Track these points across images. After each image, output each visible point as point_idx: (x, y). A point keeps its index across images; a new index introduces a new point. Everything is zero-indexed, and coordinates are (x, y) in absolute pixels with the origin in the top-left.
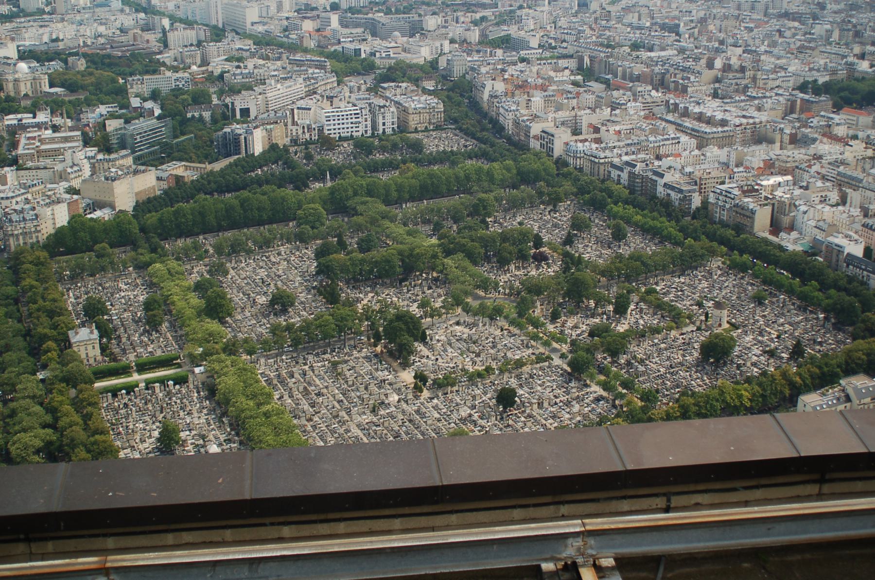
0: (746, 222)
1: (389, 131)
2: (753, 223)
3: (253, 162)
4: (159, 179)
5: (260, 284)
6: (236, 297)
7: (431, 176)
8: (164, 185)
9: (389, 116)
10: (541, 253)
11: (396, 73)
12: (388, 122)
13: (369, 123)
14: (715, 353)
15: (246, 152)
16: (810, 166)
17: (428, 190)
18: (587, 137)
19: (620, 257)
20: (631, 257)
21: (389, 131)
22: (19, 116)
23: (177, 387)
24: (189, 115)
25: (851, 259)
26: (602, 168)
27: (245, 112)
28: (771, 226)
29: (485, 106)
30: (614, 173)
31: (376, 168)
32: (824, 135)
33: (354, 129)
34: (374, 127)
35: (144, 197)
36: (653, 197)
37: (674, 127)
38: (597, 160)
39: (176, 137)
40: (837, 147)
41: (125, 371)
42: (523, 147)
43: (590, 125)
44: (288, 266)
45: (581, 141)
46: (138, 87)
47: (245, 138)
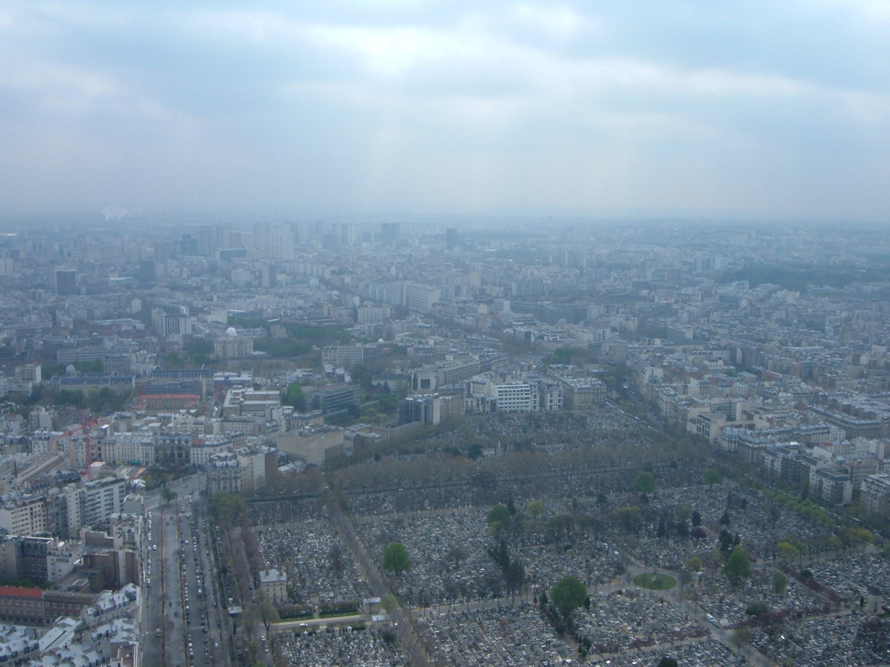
9: (556, 394)
12: (554, 401)
13: (538, 399)
15: (426, 420)
18: (741, 423)
21: (555, 408)
22: (226, 374)
23: (355, 632)
26: (756, 453)
27: (426, 384)
29: (644, 390)
34: (542, 404)
38: (751, 445)
45: (736, 427)
47: (426, 407)
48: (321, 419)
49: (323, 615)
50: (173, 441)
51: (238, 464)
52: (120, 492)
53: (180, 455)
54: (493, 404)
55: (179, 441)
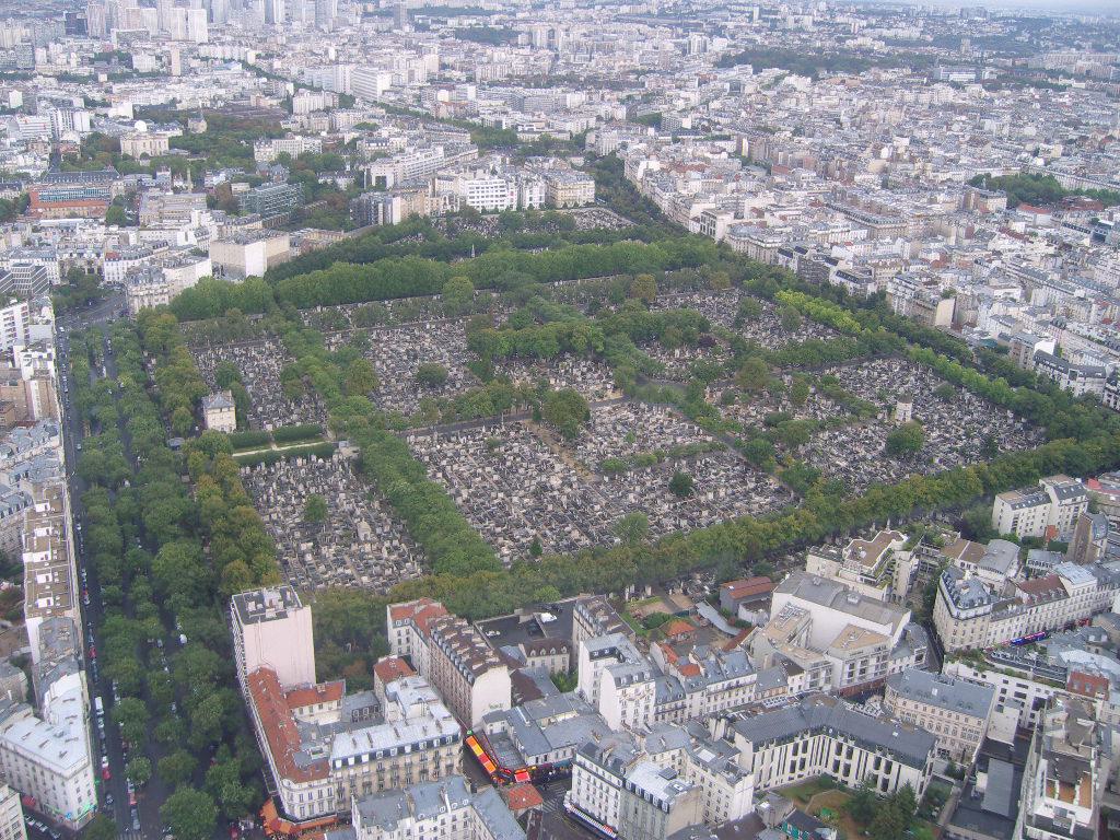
1: (536, 206)
2: (934, 316)
3: (391, 233)
4: (292, 244)
5: (405, 358)
7: (585, 252)
8: (297, 252)
9: (536, 190)
11: (545, 147)
13: (515, 198)
16: (990, 261)
19: (793, 344)
20: (806, 345)
21: (536, 206)
22: (139, 176)
23: (321, 461)
24: (321, 181)
25: (1041, 357)
27: (382, 180)
31: (524, 245)
32: (1002, 230)
35: (275, 263)
36: (827, 285)
37: (842, 215)
39: (308, 203)
40: (1018, 244)
41: (264, 441)
42: (681, 231)
43: (754, 210)
44: (437, 344)
48: (259, 225)
52: (23, 315)
53: (91, 271)
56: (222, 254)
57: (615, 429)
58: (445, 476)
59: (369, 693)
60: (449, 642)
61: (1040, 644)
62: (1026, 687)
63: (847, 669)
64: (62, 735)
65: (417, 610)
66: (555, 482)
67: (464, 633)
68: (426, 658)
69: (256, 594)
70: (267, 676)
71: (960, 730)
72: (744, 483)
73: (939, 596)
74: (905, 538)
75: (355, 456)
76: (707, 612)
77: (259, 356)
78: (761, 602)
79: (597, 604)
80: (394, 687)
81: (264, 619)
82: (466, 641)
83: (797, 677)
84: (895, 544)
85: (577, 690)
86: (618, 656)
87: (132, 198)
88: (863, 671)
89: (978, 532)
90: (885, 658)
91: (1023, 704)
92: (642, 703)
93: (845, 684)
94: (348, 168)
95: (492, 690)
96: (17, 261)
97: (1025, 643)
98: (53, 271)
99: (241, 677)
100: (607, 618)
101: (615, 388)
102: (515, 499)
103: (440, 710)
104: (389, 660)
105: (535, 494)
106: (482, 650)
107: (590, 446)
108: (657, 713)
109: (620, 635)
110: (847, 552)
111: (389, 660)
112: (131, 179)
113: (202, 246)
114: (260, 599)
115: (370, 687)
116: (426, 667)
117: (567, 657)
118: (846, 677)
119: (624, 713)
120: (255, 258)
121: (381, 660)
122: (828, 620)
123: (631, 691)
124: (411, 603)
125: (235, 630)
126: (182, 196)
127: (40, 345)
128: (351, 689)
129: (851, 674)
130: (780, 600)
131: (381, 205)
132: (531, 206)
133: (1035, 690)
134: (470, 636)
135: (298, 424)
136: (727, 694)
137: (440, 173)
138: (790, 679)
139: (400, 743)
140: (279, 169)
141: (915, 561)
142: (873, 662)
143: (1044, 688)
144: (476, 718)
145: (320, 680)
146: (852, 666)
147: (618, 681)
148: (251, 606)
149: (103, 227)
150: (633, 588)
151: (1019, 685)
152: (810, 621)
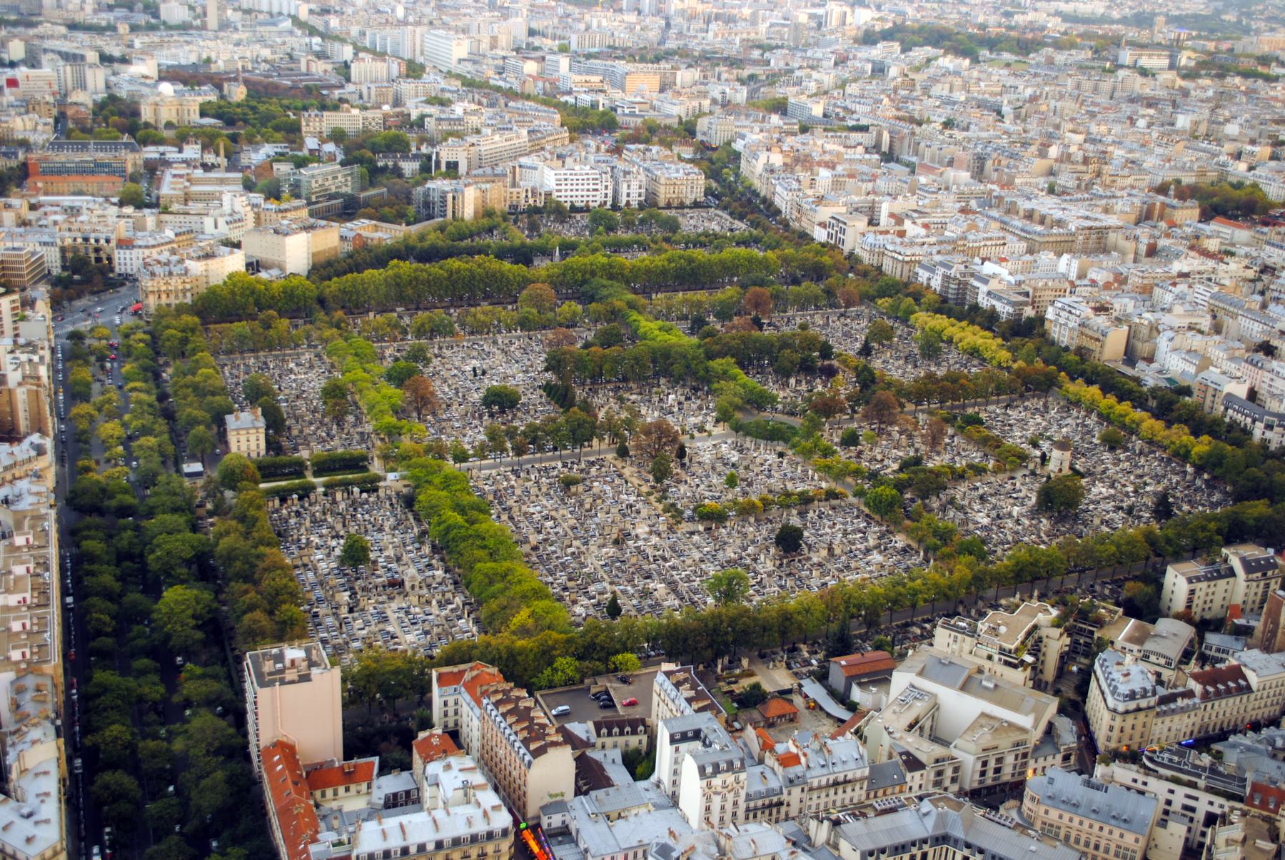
0: (1093, 346)
4: (343, 238)
5: (471, 377)
6: (441, 390)
7: (690, 260)
8: (348, 247)
9: (635, 185)
10: (831, 366)
11: (650, 133)
12: (632, 192)
13: (610, 192)
14: (1059, 501)
16: (1174, 284)
17: (691, 277)
19: (930, 376)
20: (946, 378)
21: (635, 204)
22: (161, 149)
23: (365, 495)
24: (380, 164)
25: (1230, 400)
27: (453, 166)
28: (1125, 354)
29: (758, 184)
30: (923, 275)
31: (618, 247)
32: (1192, 248)
33: (591, 199)
34: (615, 198)
35: (322, 259)
36: (975, 308)
37: (998, 225)
38: (900, 258)
39: (363, 189)
40: (1211, 263)
42: (805, 237)
43: (892, 215)
45: (881, 233)
46: (315, 126)
47: (454, 198)
49: (316, 474)
50: (86, 240)
51: (187, 271)
53: (98, 260)
54: (548, 194)
55: (97, 241)
56: (258, 246)
57: (714, 468)
58: (511, 518)
59: (406, 774)
60: (504, 715)
61: (1216, 747)
62: (1196, 799)
63: (979, 767)
64: (30, 815)
65: (468, 676)
66: (642, 530)
67: (522, 704)
68: (476, 734)
69: (275, 651)
70: (286, 750)
71: (1113, 849)
72: (865, 539)
73: (1093, 684)
74: (1055, 612)
75: (405, 491)
76: (814, 690)
77: (296, 369)
78: (881, 678)
79: (681, 676)
80: (434, 768)
81: (283, 682)
82: (523, 715)
83: (917, 774)
84: (1041, 618)
85: (654, 778)
86: (704, 744)
87: (153, 170)
88: (997, 771)
89: (1147, 609)
90: (1025, 755)
91: (1191, 820)
92: (730, 797)
93: (976, 785)
94: (414, 150)
95: (552, 772)
96: (9, 245)
97: (1203, 742)
98: (53, 259)
99: (253, 750)
100: (692, 693)
101: (718, 421)
102: (592, 548)
103: (489, 798)
104: (432, 736)
105: (616, 542)
106: (543, 726)
107: (683, 488)
108: (748, 810)
109: (708, 714)
110: (982, 626)
111: (432, 736)
112: (151, 152)
113: (235, 236)
114: (280, 658)
115: (406, 766)
116: (476, 744)
117: (644, 738)
118: (977, 777)
119: (708, 809)
120: (297, 251)
121: (422, 735)
122: (961, 707)
123: (717, 781)
124: (462, 667)
125: (249, 696)
126: (212, 175)
127: (31, 347)
128: (384, 770)
129: (983, 774)
130: (901, 679)
131: (450, 196)
132: (628, 203)
133: (1205, 803)
134: (528, 709)
135: (340, 450)
136: (832, 791)
137: (523, 160)
138: (909, 776)
139: (439, 837)
140: (330, 147)
141: (1068, 641)
142: (1010, 759)
143: (1218, 800)
144: (532, 810)
145: (348, 755)
146: (985, 764)
147: (702, 770)
148: (268, 666)
149: (115, 209)
150: (726, 659)
151: (1188, 796)
152: (936, 707)
